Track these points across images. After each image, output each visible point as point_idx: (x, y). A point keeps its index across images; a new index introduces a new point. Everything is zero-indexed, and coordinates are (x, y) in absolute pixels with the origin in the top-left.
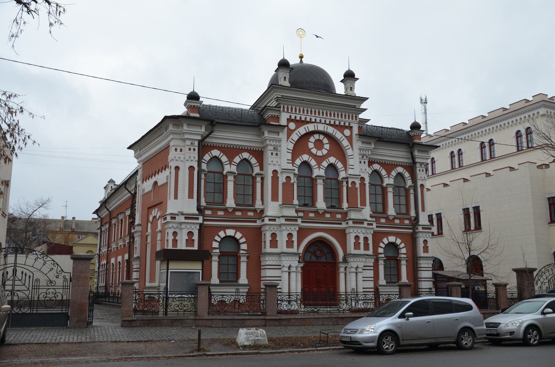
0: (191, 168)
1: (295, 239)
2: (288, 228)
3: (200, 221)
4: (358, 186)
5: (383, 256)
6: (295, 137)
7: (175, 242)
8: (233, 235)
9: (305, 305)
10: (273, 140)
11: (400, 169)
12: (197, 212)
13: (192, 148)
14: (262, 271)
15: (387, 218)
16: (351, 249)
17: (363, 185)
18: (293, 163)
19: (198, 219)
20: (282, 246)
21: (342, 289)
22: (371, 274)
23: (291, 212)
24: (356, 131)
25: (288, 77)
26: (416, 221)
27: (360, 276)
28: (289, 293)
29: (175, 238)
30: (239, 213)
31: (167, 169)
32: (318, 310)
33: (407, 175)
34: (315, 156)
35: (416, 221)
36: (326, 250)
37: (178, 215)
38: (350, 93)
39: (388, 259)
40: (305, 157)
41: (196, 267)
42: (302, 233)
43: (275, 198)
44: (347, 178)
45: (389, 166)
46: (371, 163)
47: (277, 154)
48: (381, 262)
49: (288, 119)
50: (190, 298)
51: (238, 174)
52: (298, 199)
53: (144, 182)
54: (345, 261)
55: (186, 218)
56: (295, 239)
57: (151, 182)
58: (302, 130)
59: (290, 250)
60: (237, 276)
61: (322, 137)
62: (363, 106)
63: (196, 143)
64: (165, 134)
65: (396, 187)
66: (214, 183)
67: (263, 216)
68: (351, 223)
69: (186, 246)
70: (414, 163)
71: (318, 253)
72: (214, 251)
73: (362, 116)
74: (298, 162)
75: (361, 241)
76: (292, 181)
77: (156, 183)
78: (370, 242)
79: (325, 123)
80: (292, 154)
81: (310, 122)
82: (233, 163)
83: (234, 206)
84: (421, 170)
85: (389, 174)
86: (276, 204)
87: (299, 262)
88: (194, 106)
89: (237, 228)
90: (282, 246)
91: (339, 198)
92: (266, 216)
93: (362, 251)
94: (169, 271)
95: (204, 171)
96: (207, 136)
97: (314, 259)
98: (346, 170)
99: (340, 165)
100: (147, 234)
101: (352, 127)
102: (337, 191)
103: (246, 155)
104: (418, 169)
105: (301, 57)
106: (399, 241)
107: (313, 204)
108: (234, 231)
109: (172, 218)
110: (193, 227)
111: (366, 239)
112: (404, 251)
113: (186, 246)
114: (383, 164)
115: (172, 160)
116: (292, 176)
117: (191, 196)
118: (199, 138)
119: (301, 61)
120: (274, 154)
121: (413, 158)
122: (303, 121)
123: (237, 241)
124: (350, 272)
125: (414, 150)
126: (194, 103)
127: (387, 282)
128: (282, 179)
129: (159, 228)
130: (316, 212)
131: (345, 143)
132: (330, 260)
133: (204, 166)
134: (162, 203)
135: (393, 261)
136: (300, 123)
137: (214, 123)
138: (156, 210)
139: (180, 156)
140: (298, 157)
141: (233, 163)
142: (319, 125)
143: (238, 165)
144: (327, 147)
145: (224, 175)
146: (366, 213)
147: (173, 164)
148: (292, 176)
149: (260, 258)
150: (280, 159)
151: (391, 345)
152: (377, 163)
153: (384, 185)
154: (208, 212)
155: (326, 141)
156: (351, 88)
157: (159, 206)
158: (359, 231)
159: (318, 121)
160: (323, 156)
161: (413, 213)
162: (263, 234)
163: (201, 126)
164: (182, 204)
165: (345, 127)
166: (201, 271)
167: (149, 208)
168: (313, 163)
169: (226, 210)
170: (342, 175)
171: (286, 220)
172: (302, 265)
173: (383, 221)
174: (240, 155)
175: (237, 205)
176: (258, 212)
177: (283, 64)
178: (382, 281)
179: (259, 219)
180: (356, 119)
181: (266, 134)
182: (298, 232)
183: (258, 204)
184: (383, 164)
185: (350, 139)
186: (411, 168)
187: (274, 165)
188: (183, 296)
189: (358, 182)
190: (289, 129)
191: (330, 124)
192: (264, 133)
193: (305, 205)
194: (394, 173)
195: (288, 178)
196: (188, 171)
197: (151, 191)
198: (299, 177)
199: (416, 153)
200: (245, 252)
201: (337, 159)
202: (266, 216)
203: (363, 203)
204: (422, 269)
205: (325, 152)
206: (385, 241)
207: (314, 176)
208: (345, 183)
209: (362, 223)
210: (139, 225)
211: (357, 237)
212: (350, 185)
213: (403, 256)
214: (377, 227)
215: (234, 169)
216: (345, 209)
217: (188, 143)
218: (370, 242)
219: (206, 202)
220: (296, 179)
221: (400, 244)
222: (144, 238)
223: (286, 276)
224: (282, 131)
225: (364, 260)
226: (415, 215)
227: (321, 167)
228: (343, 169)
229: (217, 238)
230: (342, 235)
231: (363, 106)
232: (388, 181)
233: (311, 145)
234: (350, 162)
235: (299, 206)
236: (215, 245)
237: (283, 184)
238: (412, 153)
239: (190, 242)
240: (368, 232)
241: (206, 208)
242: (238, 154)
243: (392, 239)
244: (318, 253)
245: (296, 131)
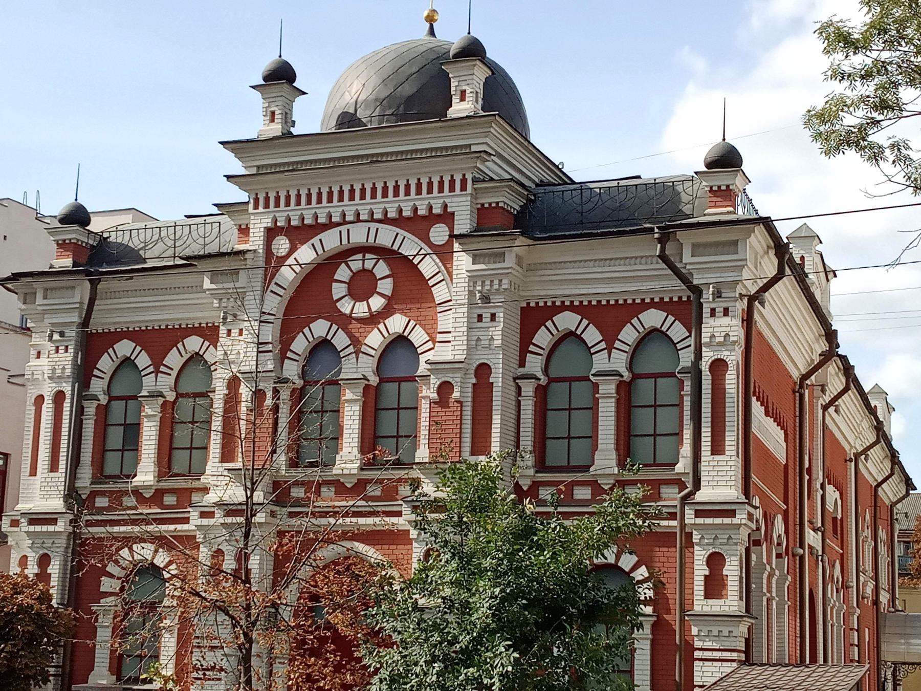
0: (59, 397)
19: (54, 521)
24: (463, 224)
33: (677, 331)
40: (320, 328)
45: (610, 316)
58: (306, 254)
63: (71, 333)
74: (300, 344)
79: (373, 220)
81: (330, 225)
82: (162, 369)
85: (610, 338)
88: (64, 241)
89: (161, 542)
105: (431, 19)
117: (54, 467)
118: (75, 318)
126: (73, 233)
131: (428, 267)
136: (300, 233)
141: (162, 369)
144: (386, 286)
152: (572, 308)
155: (382, 269)
161: (683, 466)
165: (432, 219)
168: (341, 340)
180: (464, 188)
185: (444, 253)
191: (386, 220)
204: (734, 655)
205: (377, 303)
233: (338, 290)
238: (663, 257)
241: (93, 495)
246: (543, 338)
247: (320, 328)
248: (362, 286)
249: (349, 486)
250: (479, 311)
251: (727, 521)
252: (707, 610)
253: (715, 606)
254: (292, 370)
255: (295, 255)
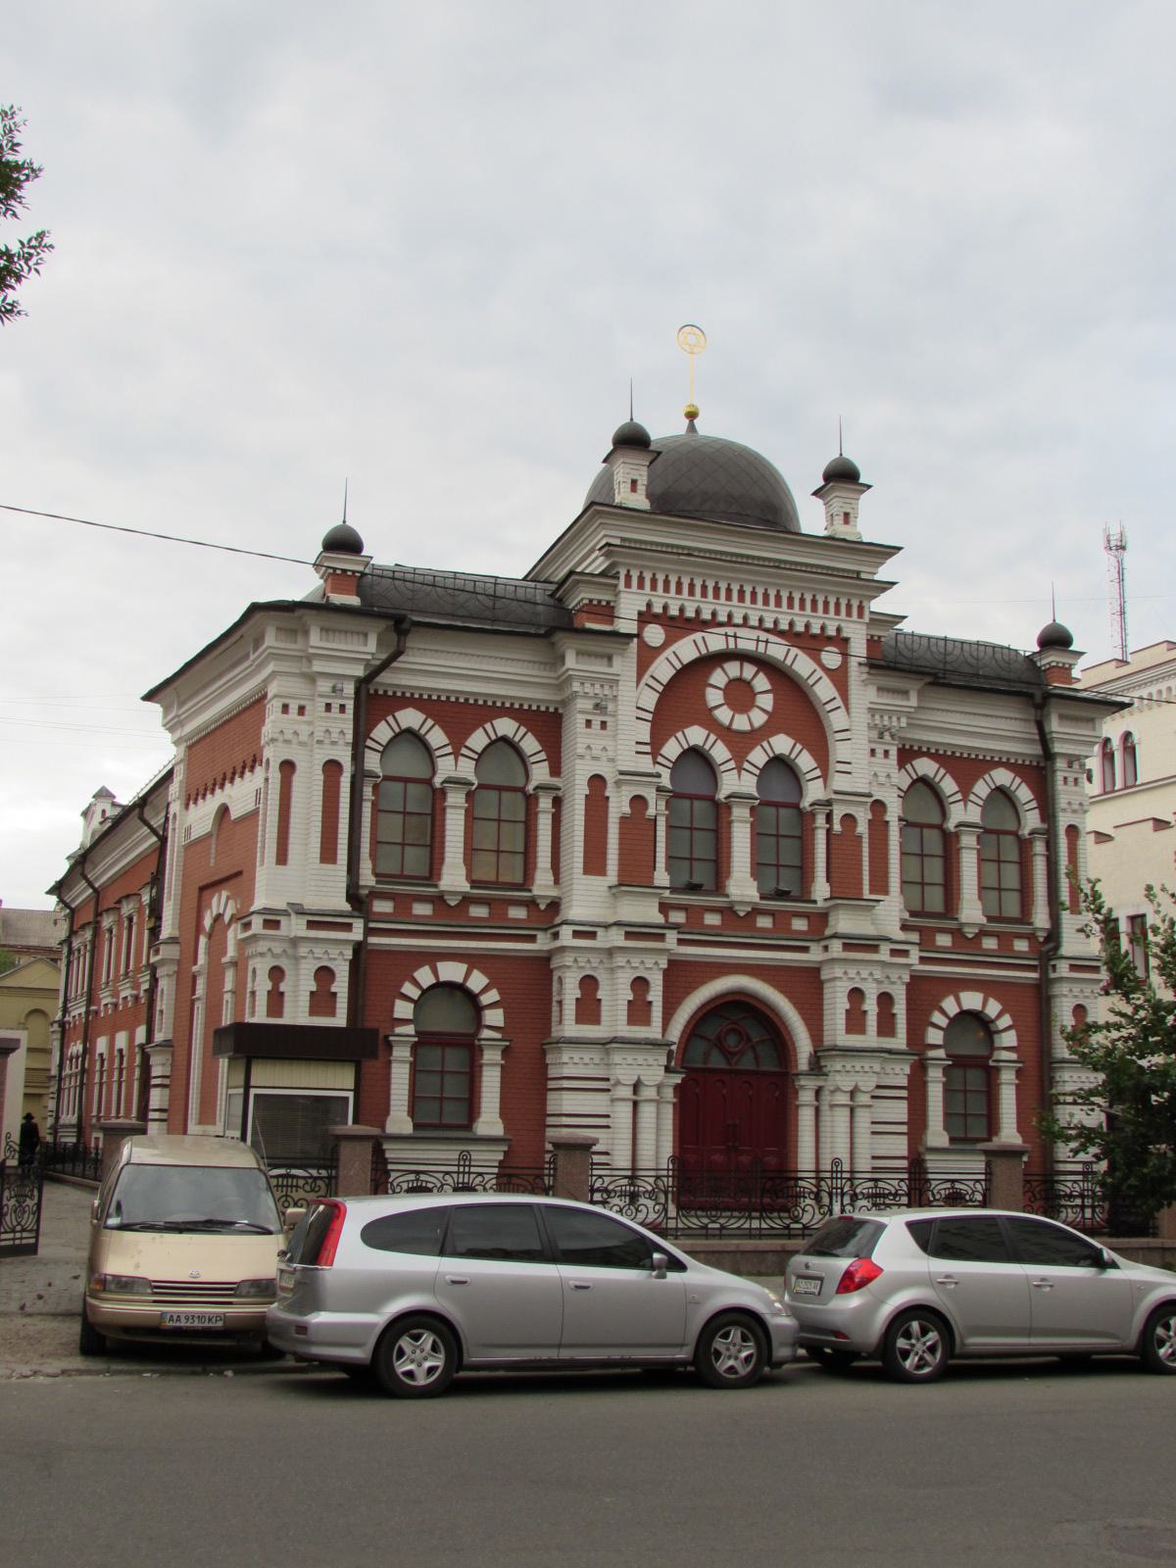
0: (332, 767)
1: (656, 995)
2: (636, 961)
3: (357, 933)
4: (862, 828)
5: (941, 1053)
6: (663, 670)
7: (276, 1000)
8: (459, 979)
9: (680, 1207)
10: (593, 681)
11: (1002, 777)
12: (347, 907)
13: (336, 704)
14: (551, 1096)
15: (957, 933)
16: (836, 1030)
17: (879, 825)
18: (655, 753)
19: (348, 927)
20: (614, 1019)
21: (805, 1160)
22: (899, 1111)
23: (644, 910)
24: (859, 648)
25: (643, 481)
26: (1051, 945)
27: (863, 1119)
28: (634, 1169)
29: (276, 986)
30: (479, 912)
31: (258, 769)
32: (723, 1227)
33: (1024, 794)
34: (726, 733)
35: (1051, 945)
36: (756, 1034)
37: (285, 913)
38: (842, 531)
39: (958, 1064)
40: (696, 735)
41: (336, 1081)
42: (680, 977)
43: (594, 864)
44: (829, 803)
45: (967, 767)
46: (906, 755)
47: (604, 725)
48: (935, 1078)
49: (640, 614)
50: (316, 1179)
51: (481, 786)
52: (668, 869)
53: (192, 806)
54: (817, 1067)
55: (311, 925)
56: (656, 995)
57: (209, 806)
58: (687, 649)
59: (640, 1032)
60: (472, 1109)
61: (749, 671)
62: (883, 573)
63: (349, 689)
64: (252, 657)
65: (987, 831)
66: (405, 813)
67: (558, 920)
68: (836, 946)
69: (313, 1012)
70: (1049, 756)
71: (731, 1041)
72: (399, 1030)
73: (881, 604)
74: (672, 749)
75: (871, 1006)
76: (651, 812)
77: (224, 810)
78: (900, 1009)
79: (761, 627)
80: (654, 724)
82: (464, 751)
83: (466, 887)
84: (1071, 780)
85: (965, 789)
86: (601, 884)
87: (668, 1069)
88: (344, 571)
90: (614, 1019)
91: (801, 868)
92: (565, 923)
93: (870, 1038)
94: (253, 1092)
95: (372, 775)
96: (385, 665)
97: (717, 1061)
98: (825, 776)
99: (805, 762)
100: (195, 969)
101: (846, 640)
102: (797, 842)
103: (506, 726)
104: (1059, 776)
105: (692, 416)
106: (993, 1008)
107: (719, 888)
108: (464, 967)
109: (268, 924)
110: (334, 952)
111: (885, 999)
112: (1009, 1039)
113: (313, 1012)
114: (950, 761)
115: (273, 740)
116: (650, 794)
117: (328, 855)
118: (359, 671)
119: (692, 428)
120: (596, 724)
121: (1044, 740)
122: (688, 620)
123: (472, 998)
124: (832, 1106)
125: (1049, 715)
126: (345, 562)
127: (952, 1140)
128: (619, 805)
129: (231, 952)
130: (728, 912)
131: (824, 690)
132: (769, 1066)
133: (372, 761)
134: (239, 874)
135: (973, 1069)
136: (679, 626)
137: (405, 626)
138: (224, 894)
139: (296, 727)
140: (672, 733)
141: (464, 751)
142: (741, 632)
143: (480, 758)
144: (766, 701)
145: (434, 791)
146: (889, 914)
147: (273, 754)
148: (650, 794)
149: (544, 1053)
150: (614, 742)
151: (427, 1364)
152: (928, 754)
153: (951, 825)
154: (382, 907)
155: (762, 683)
156: (846, 515)
157: (232, 882)
158: (865, 974)
159: (738, 620)
160: (753, 731)
161: (1041, 919)
162: (555, 978)
163: (366, 635)
164: (301, 879)
166: (351, 1095)
167: (202, 889)
168: (720, 753)
169: (438, 900)
170: (814, 791)
171: (629, 935)
172: (677, 1079)
173: (944, 940)
174: (488, 726)
175: (474, 884)
176: (542, 907)
177: (631, 440)
178: (937, 1134)
179: (546, 930)
180: (861, 615)
181: (571, 661)
182: (666, 973)
183: (543, 885)
184: (950, 761)
185: (839, 678)
186: (1040, 773)
187: (594, 758)
188: (294, 1172)
189: (863, 816)
190: (644, 646)
192: (562, 659)
193: (693, 888)
194: (982, 789)
195: (638, 801)
196: (320, 777)
197: (209, 836)
198: (674, 797)
199: (1055, 725)
200: (498, 1035)
201: (798, 740)
202: (565, 923)
203: (880, 885)
205: (759, 719)
206: (950, 1006)
207: (721, 796)
208: (821, 820)
209: (875, 949)
210: (173, 940)
211: (856, 995)
212: (837, 827)
213: (1005, 1055)
214: (923, 960)
215: (466, 769)
216: (820, 904)
217: (324, 686)
218: (900, 1009)
219: (376, 875)
220: (662, 804)
221: (999, 1015)
222: (186, 983)
223: (623, 1110)
224: (623, 653)
225: (877, 1067)
226: (1047, 925)
227: (746, 765)
228: (818, 773)
229: (408, 989)
230: (807, 986)
231: (883, 573)
232: (963, 813)
233: (714, 697)
234: (840, 751)
235: (673, 890)
236: (403, 1010)
237: (623, 820)
239: (322, 1000)
240: (894, 977)
241: (375, 894)
242: (480, 724)
243: (972, 1000)
244: (731, 1041)
245: (668, 653)
247: (696, 735)
248: (740, 695)
249: (742, 914)
250: (874, 746)
255: (674, 647)
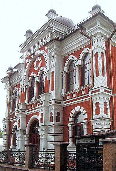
17: (53, 76)
144: (40, 62)
146: (53, 95)
206: (73, 111)
243: (77, 109)
246: (67, 63)
251: (98, 93)
252: (96, 118)
253: (98, 116)
254: (29, 84)
